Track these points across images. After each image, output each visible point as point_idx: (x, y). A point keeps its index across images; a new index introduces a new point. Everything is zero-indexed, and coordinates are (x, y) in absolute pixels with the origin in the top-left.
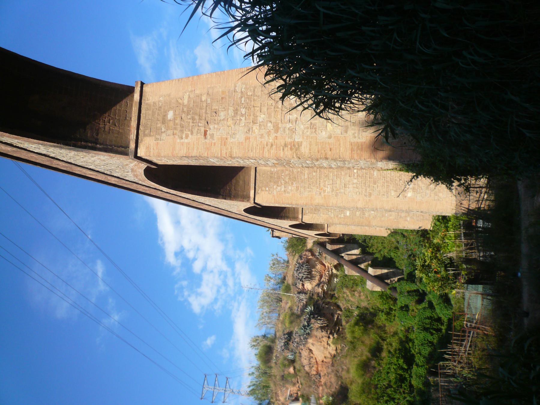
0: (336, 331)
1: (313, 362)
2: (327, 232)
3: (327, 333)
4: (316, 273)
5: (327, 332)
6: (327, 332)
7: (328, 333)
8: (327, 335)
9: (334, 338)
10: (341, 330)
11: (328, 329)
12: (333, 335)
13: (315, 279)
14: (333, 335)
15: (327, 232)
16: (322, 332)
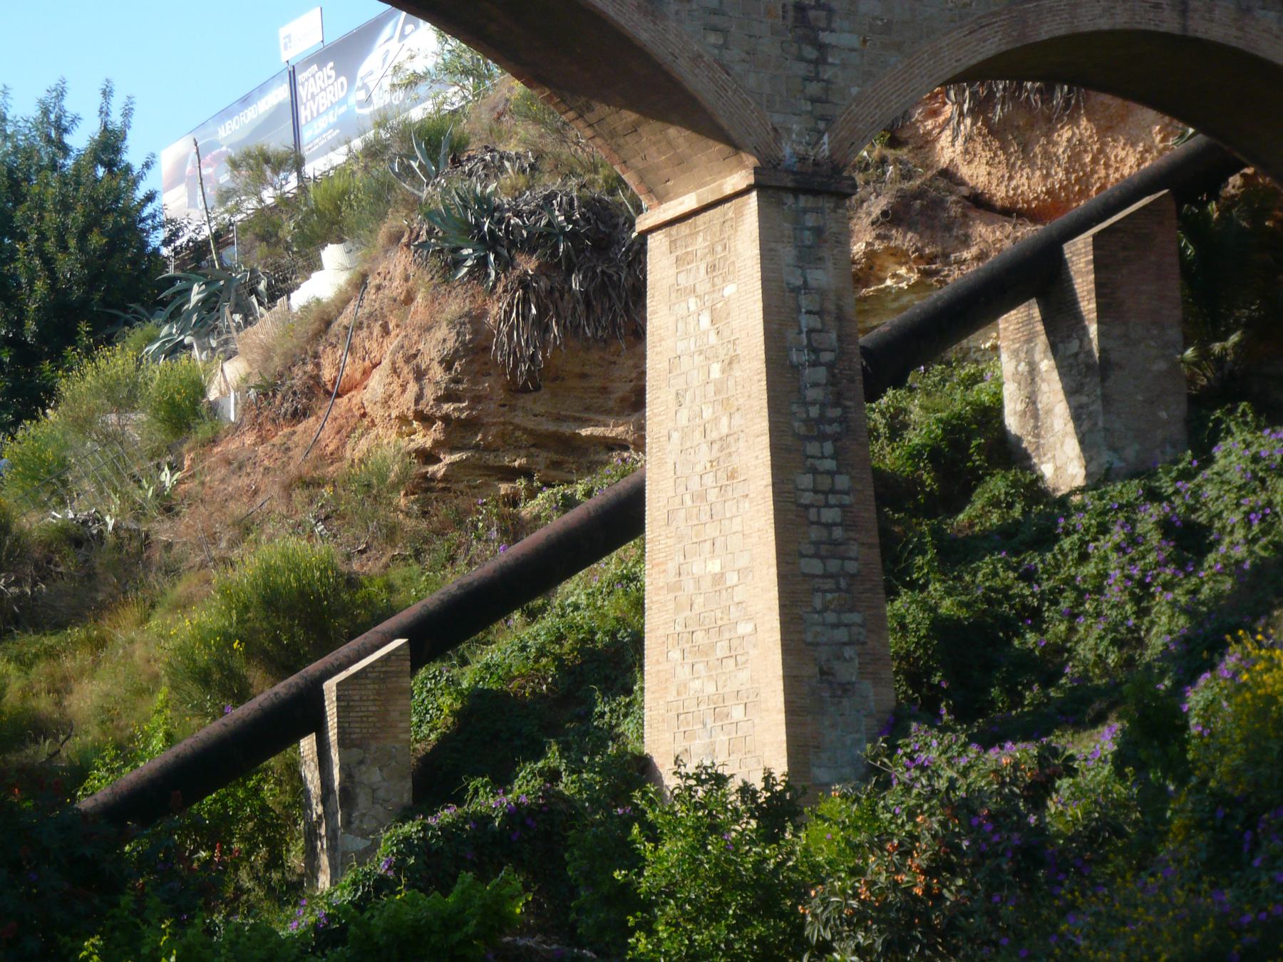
0: (490, 459)
1: (372, 345)
2: (644, 235)
3: (439, 400)
4: (1064, 159)
5: (449, 397)
6: (449, 397)
7: (448, 407)
8: (427, 405)
9: (428, 456)
10: (504, 488)
11: (476, 400)
12: (447, 444)
13: (1011, 167)
14: (447, 444)
15: (644, 235)
16: (447, 364)
